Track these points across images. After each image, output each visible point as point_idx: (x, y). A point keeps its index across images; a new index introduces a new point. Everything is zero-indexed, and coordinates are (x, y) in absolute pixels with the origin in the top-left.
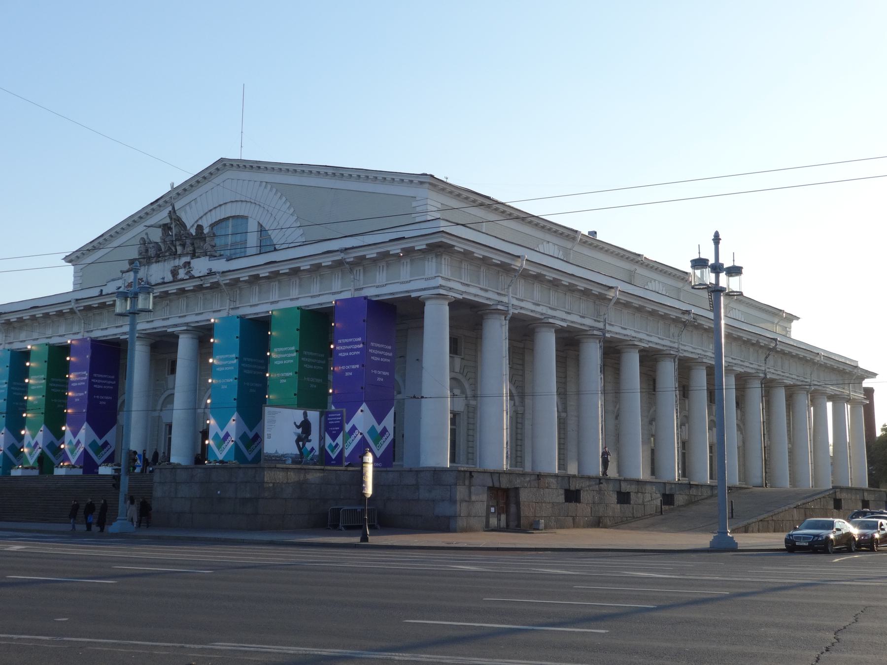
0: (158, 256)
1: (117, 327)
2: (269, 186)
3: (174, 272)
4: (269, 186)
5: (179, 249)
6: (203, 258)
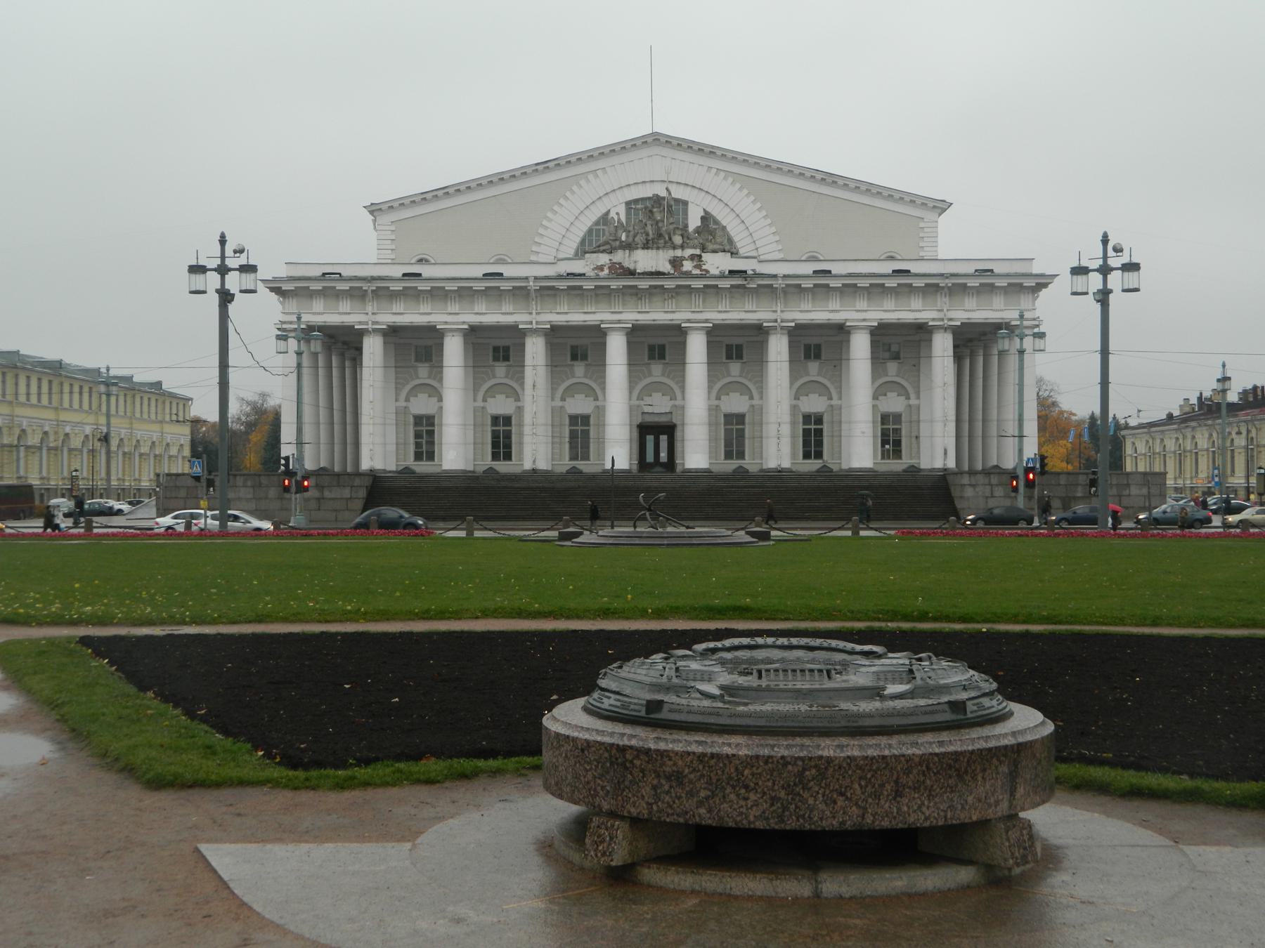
0: (648, 241)
2: (722, 175)
3: (676, 263)
4: (722, 175)
5: (678, 240)
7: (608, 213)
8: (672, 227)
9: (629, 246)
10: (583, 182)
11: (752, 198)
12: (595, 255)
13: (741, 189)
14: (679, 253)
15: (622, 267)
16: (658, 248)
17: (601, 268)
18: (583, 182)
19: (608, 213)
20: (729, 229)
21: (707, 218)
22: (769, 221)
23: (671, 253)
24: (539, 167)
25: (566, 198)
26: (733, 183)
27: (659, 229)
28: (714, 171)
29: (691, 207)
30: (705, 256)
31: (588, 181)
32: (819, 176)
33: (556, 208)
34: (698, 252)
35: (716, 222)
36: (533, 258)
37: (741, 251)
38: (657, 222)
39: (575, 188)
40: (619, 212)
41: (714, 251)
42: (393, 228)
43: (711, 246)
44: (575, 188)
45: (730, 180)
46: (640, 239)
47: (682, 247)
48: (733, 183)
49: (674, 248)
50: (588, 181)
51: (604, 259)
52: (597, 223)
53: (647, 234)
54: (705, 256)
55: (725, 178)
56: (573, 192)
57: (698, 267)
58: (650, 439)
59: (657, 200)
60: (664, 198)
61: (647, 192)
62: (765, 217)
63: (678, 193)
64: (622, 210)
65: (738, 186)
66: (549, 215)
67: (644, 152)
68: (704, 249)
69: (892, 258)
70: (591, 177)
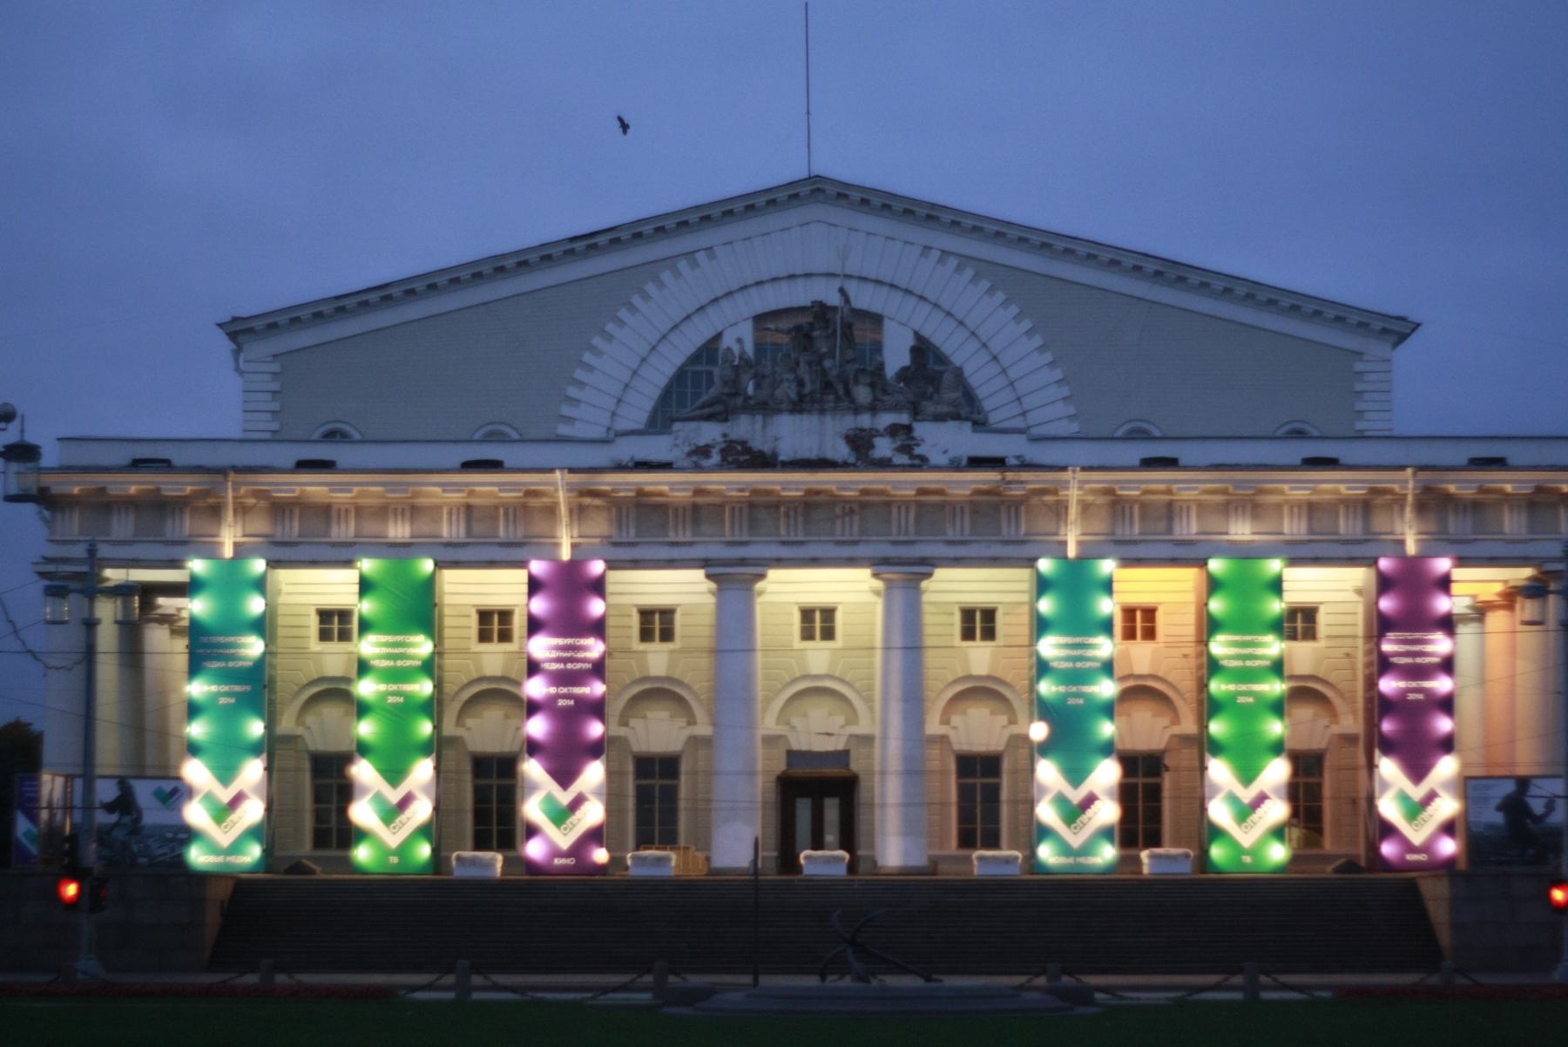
0: (801, 397)
1: (673, 544)
2: (953, 262)
3: (860, 443)
4: (953, 262)
5: (863, 394)
6: (951, 425)
7: (718, 336)
8: (851, 368)
9: (766, 408)
10: (666, 276)
11: (1014, 310)
12: (692, 425)
13: (991, 291)
14: (865, 421)
15: (747, 450)
16: (822, 412)
17: (704, 451)
18: (666, 276)
19: (718, 336)
20: (968, 371)
21: (922, 349)
22: (1048, 357)
23: (849, 422)
24: (577, 245)
25: (632, 308)
26: (976, 278)
27: (824, 372)
28: (935, 254)
29: (889, 328)
30: (922, 429)
31: (677, 274)
32: (1151, 267)
33: (610, 327)
34: (904, 418)
35: (942, 359)
36: (564, 430)
37: (994, 418)
38: (821, 358)
39: (650, 288)
40: (740, 338)
41: (939, 418)
42: (275, 367)
43: (930, 408)
44: (650, 288)
45: (969, 273)
46: (787, 390)
47: (873, 409)
48: (976, 278)
49: (857, 410)
50: (677, 274)
51: (710, 433)
52: (695, 358)
53: (801, 384)
54: (922, 429)
55: (959, 269)
56: (646, 297)
57: (906, 449)
58: (803, 808)
59: (821, 311)
60: (834, 309)
61: (800, 294)
62: (1042, 349)
63: (864, 298)
64: (746, 332)
65: (985, 284)
66: (597, 341)
67: (793, 216)
68: (916, 413)
69: (1298, 435)
70: (683, 265)
